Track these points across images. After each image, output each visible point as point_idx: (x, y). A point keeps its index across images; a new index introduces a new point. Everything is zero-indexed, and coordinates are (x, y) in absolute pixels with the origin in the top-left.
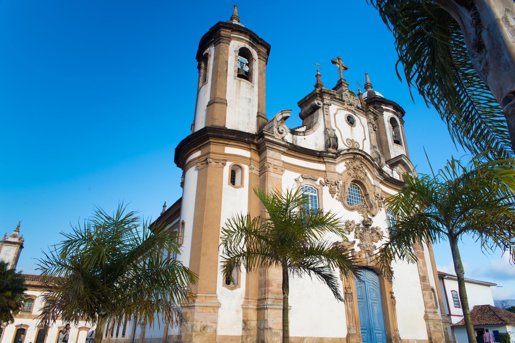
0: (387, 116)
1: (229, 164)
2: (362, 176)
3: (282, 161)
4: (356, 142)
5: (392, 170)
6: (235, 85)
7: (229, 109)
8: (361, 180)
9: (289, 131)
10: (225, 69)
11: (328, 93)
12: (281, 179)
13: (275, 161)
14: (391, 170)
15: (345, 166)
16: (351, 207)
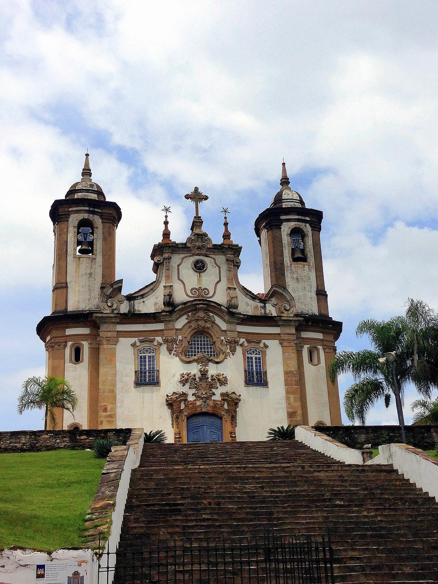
0: (286, 228)
1: (69, 344)
2: (208, 325)
3: (115, 331)
4: (205, 289)
5: (265, 304)
6: (74, 263)
7: (69, 290)
10: (65, 250)
11: (167, 247)
14: (263, 305)
15: (186, 319)
16: (188, 360)
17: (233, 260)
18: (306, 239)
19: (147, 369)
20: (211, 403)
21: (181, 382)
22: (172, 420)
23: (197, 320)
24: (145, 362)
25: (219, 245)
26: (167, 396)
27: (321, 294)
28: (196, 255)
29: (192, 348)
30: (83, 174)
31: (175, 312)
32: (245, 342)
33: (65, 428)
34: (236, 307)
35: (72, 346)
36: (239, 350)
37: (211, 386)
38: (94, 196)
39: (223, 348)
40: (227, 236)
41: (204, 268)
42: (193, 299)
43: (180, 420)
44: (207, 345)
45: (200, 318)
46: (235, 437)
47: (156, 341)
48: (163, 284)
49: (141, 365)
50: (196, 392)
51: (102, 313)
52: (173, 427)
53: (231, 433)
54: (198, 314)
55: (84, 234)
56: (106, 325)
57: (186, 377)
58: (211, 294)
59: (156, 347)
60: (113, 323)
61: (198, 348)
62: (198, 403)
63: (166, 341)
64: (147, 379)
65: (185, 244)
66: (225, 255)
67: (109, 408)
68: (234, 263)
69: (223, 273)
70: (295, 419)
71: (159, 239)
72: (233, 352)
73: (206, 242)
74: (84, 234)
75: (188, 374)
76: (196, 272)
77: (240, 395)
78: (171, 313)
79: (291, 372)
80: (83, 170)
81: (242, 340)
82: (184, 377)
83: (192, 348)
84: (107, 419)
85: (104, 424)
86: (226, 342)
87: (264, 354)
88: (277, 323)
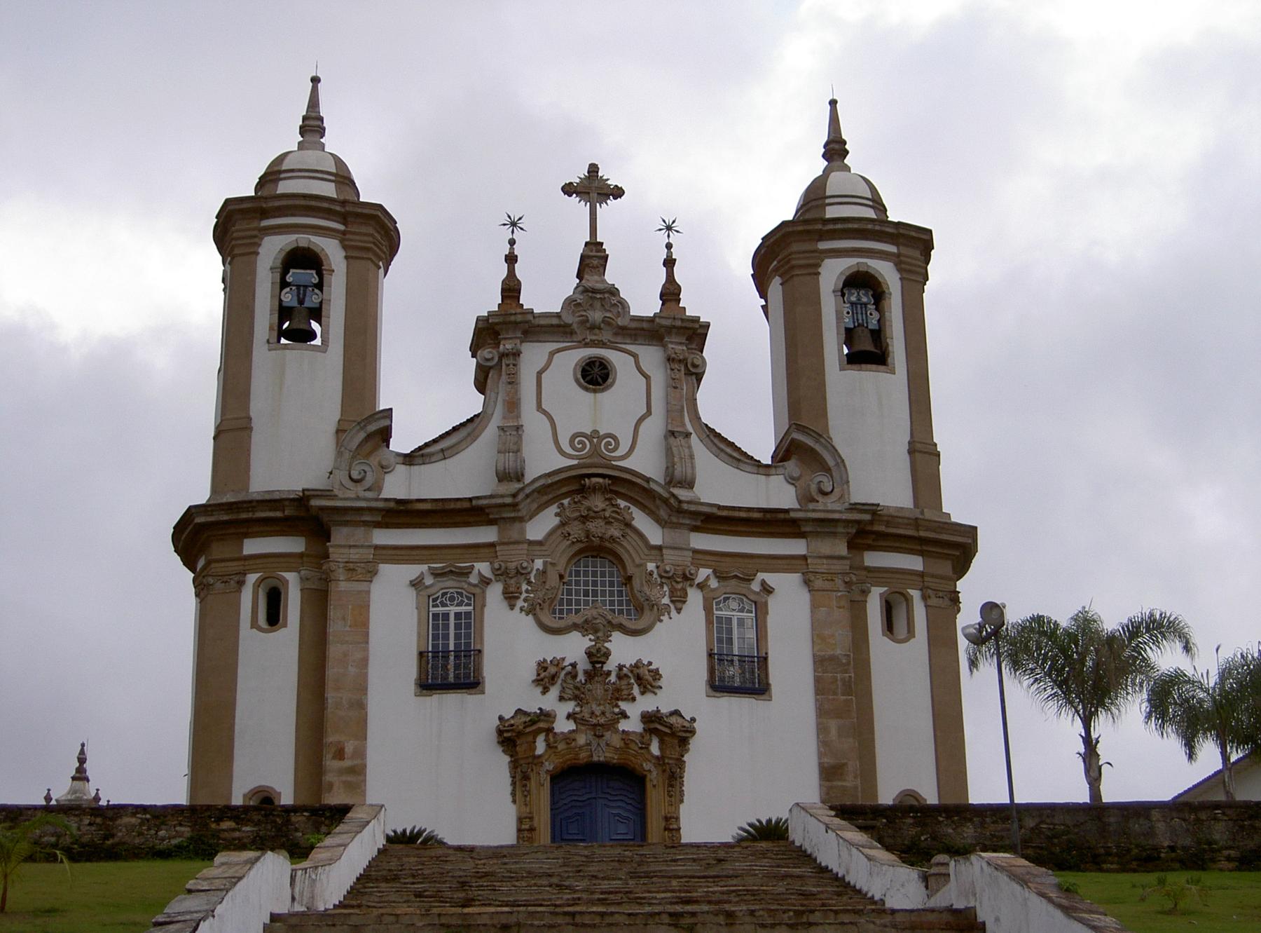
0: (832, 272)
1: (252, 578)
2: (615, 531)
3: (370, 546)
8: (607, 544)
9: (401, 459)
12: (368, 592)
13: (352, 551)
15: (557, 515)
16: (562, 624)
18: (885, 303)
19: (452, 647)
20: (616, 741)
21: (538, 681)
22: (514, 784)
23: (584, 519)
24: (446, 627)
26: (501, 718)
27: (923, 455)
28: (587, 345)
29: (569, 593)
30: (303, 130)
32: (712, 577)
33: (237, 800)
34: (690, 485)
35: (257, 585)
36: (695, 598)
37: (618, 694)
38: (328, 190)
39: (654, 593)
40: (671, 293)
41: (605, 377)
42: (575, 462)
43: (533, 784)
44: (612, 584)
45: (592, 514)
46: (679, 829)
47: (475, 571)
48: (496, 421)
49: (435, 637)
50: (578, 709)
51: (334, 497)
52: (514, 801)
53: (667, 819)
54: (586, 503)
55: (298, 287)
56: (345, 530)
57: (552, 670)
59: (477, 591)
60: (366, 524)
61: (586, 594)
62: (581, 740)
63: (501, 574)
64: (451, 675)
65: (558, 315)
66: (664, 346)
67: (349, 748)
68: (686, 366)
70: (840, 783)
71: (491, 301)
72: (679, 605)
73: (615, 311)
74: (298, 287)
75: (557, 663)
77: (693, 720)
79: (832, 658)
80: (305, 118)
81: (704, 573)
82: (545, 669)
83: (569, 593)
84: (344, 778)
85: (335, 788)
86: (661, 577)
87: (761, 611)
88: (799, 527)
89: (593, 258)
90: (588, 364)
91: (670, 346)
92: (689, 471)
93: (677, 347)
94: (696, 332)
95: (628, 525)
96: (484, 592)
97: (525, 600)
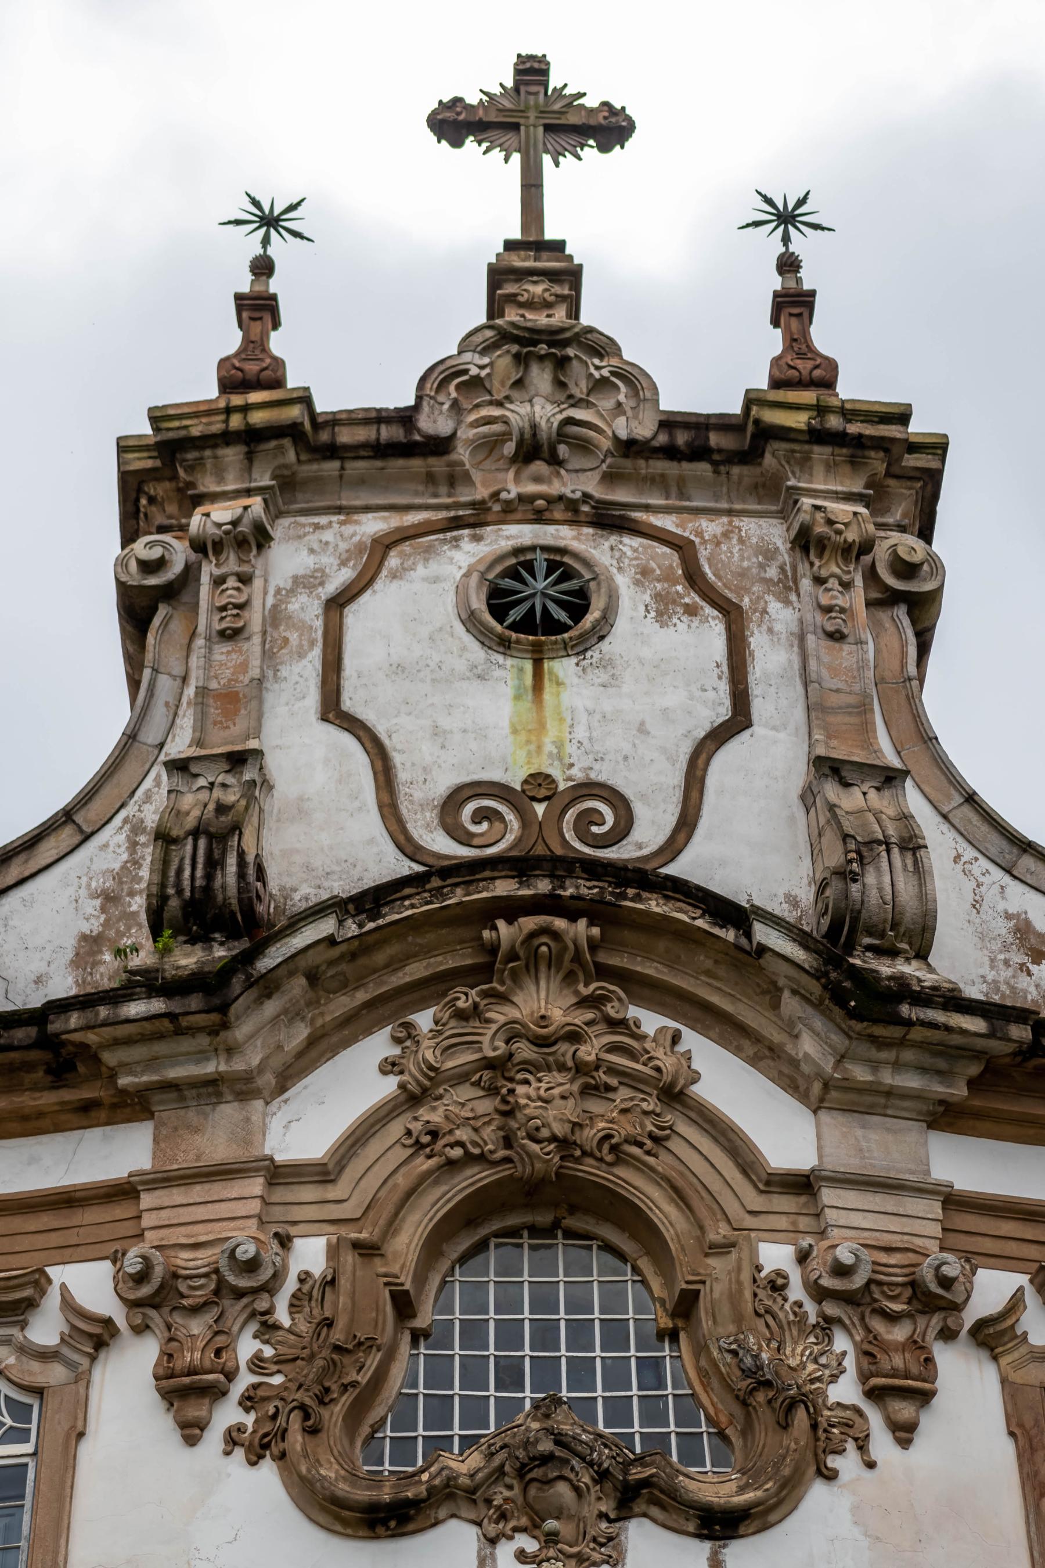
4: (590, 789)
8: (589, 1168)
15: (389, 1067)
17: (866, 547)
25: (723, 423)
28: (512, 510)
29: (438, 1374)
31: (268, 986)
32: (1031, 1297)
41: (578, 605)
45: (525, 1051)
47: (53, 1300)
54: (499, 1015)
58: (649, 833)
61: (510, 1375)
63: (154, 1297)
65: (405, 417)
68: (871, 575)
69: (770, 658)
72: (904, 1410)
73: (606, 404)
76: (504, 645)
78: (212, 996)
86: (819, 1294)
89: (534, 272)
90: (512, 573)
91: (807, 502)
92: (906, 889)
93: (830, 496)
94: (899, 463)
95: (675, 1094)
96: (82, 1379)
97: (248, 1402)
